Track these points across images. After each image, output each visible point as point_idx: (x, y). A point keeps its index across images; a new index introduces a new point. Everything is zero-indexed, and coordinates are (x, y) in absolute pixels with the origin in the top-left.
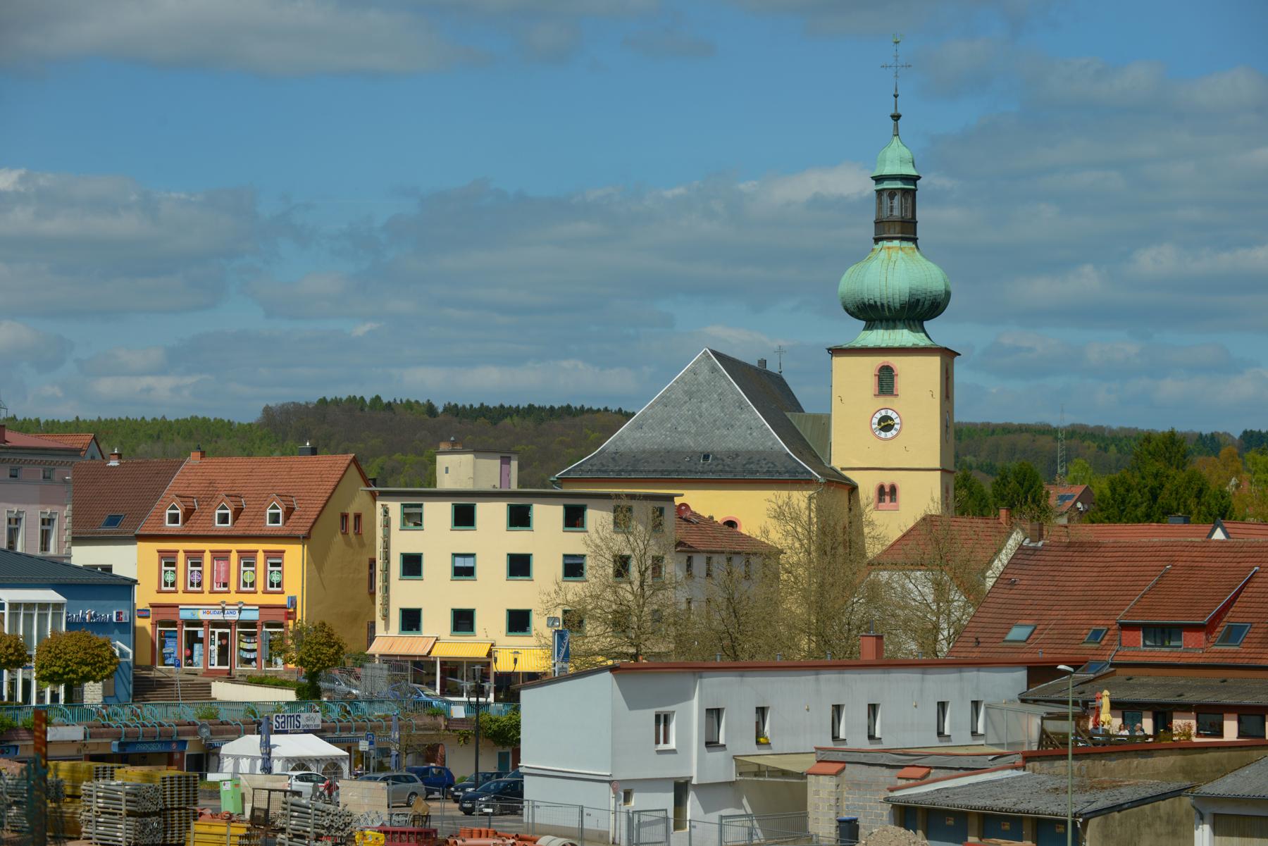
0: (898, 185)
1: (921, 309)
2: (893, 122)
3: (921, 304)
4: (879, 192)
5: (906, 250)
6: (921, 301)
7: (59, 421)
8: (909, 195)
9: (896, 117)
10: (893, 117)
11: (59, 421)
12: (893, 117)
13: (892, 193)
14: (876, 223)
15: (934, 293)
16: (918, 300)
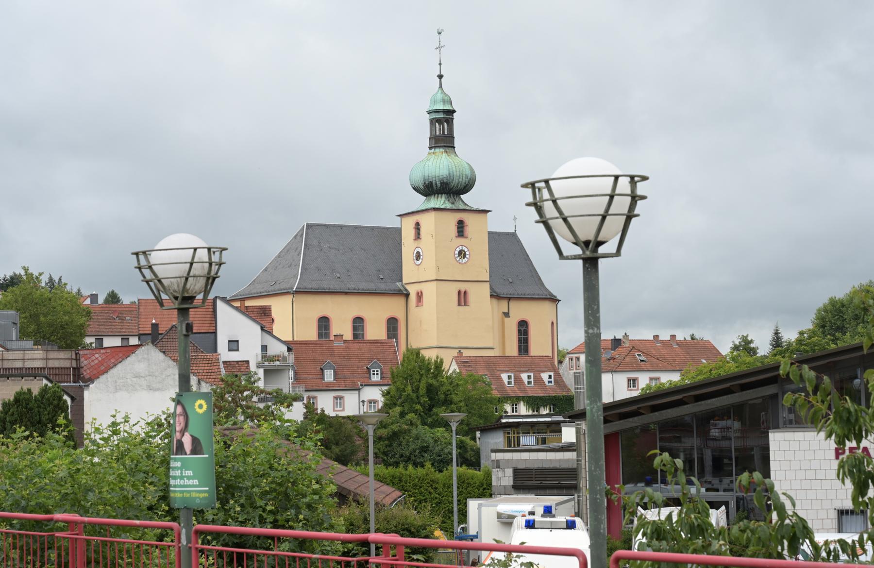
0: (441, 115)
1: (436, 186)
2: (438, 80)
3: (434, 184)
4: (431, 121)
5: (437, 154)
6: (434, 182)
7: (113, 298)
8: (450, 122)
9: (440, 77)
10: (438, 76)
11: (113, 298)
12: (438, 76)
13: (439, 121)
14: (430, 138)
15: (441, 177)
16: (431, 183)
